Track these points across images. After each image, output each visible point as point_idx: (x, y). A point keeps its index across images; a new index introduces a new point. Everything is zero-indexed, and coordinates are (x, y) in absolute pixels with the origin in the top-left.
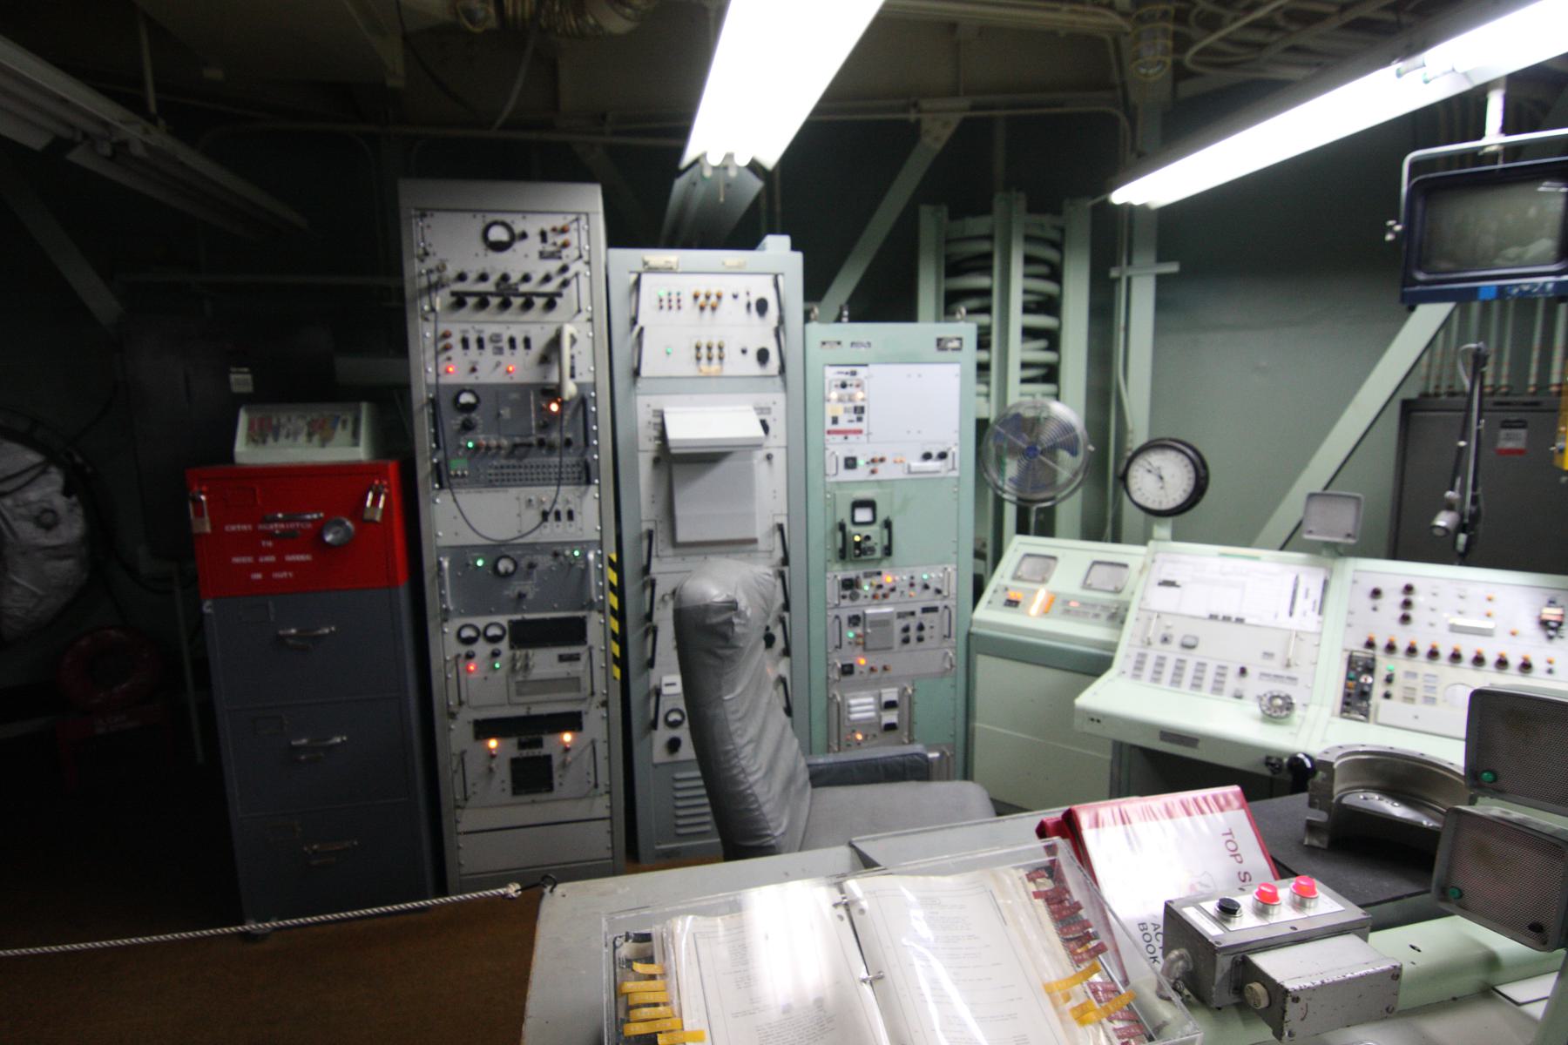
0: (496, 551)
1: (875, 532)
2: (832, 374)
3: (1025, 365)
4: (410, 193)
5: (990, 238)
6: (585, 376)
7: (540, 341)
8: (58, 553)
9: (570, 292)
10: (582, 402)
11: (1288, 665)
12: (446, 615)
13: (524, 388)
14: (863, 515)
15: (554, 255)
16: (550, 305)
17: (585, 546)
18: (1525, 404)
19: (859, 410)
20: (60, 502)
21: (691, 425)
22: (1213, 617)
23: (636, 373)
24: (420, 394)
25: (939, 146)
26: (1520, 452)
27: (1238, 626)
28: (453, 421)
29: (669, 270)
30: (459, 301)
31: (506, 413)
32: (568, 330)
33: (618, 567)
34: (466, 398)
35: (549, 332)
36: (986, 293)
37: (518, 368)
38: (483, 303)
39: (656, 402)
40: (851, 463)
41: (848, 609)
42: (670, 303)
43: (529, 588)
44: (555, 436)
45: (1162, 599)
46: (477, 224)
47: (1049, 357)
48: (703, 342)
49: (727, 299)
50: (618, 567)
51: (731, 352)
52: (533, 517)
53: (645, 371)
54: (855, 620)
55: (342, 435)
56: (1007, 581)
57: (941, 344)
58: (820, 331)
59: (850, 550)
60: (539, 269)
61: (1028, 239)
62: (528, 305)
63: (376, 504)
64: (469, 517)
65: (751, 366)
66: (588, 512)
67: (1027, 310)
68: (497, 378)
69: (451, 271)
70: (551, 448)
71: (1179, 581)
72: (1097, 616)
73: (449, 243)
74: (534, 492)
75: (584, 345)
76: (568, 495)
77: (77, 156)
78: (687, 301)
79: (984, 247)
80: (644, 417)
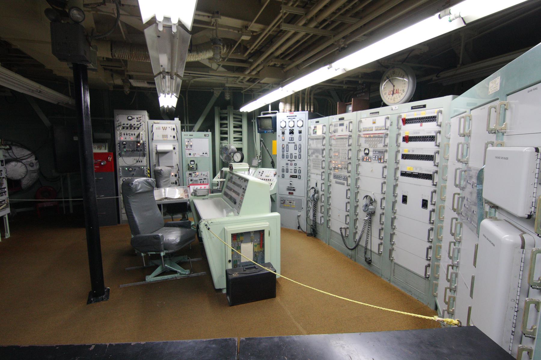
0: (129, 167)
1: (194, 166)
2: (186, 140)
3: (234, 138)
4: (116, 112)
5: (227, 114)
6: (144, 140)
7: (137, 134)
8: (33, 172)
9: (141, 127)
10: (143, 144)
12: (121, 177)
13: (134, 141)
14: (192, 163)
15: (139, 121)
16: (138, 129)
17: (144, 166)
19: (191, 146)
20: (34, 161)
21: (161, 147)
23: (153, 139)
24: (117, 142)
25: (217, 96)
28: (123, 146)
29: (158, 123)
30: (123, 128)
31: (131, 145)
32: (141, 133)
33: (150, 170)
34: (124, 143)
35: (138, 133)
36: (227, 124)
37: (133, 138)
38: (127, 128)
39: (156, 144)
40: (190, 154)
41: (190, 178)
42: (158, 128)
43: (135, 173)
44: (139, 149)
46: (127, 116)
47: (240, 136)
48: (164, 135)
49: (168, 128)
50: (150, 170)
51: (169, 136)
52: (135, 161)
53: (154, 139)
54: (191, 180)
55: (103, 148)
57: (205, 135)
58: (183, 133)
59: (190, 169)
60: (136, 123)
61: (234, 114)
62: (135, 129)
63: (110, 159)
64: (124, 162)
65: (172, 138)
66: (144, 161)
67: (234, 127)
68: (130, 140)
69: (122, 123)
70: (138, 151)
73: (122, 119)
74: (135, 158)
75: (144, 135)
76: (141, 158)
77: (60, 104)
78: (161, 128)
79: (226, 115)
80: (154, 146)
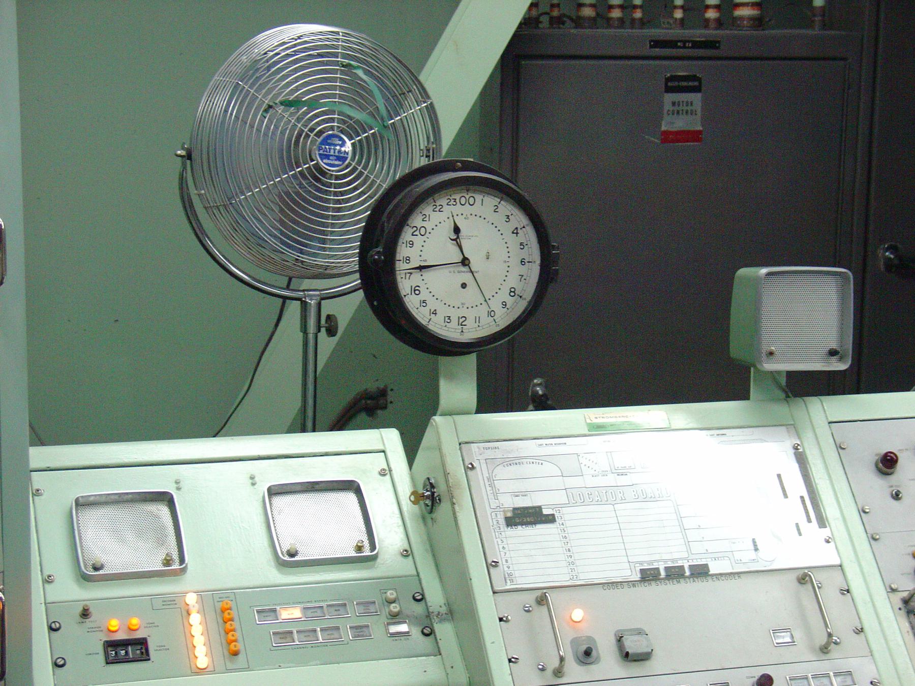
11: (824, 650)
18: (696, 45)
22: (649, 576)
26: (695, 136)
27: (700, 585)
45: (530, 558)
56: (67, 590)
71: (545, 501)
72: (360, 631)
